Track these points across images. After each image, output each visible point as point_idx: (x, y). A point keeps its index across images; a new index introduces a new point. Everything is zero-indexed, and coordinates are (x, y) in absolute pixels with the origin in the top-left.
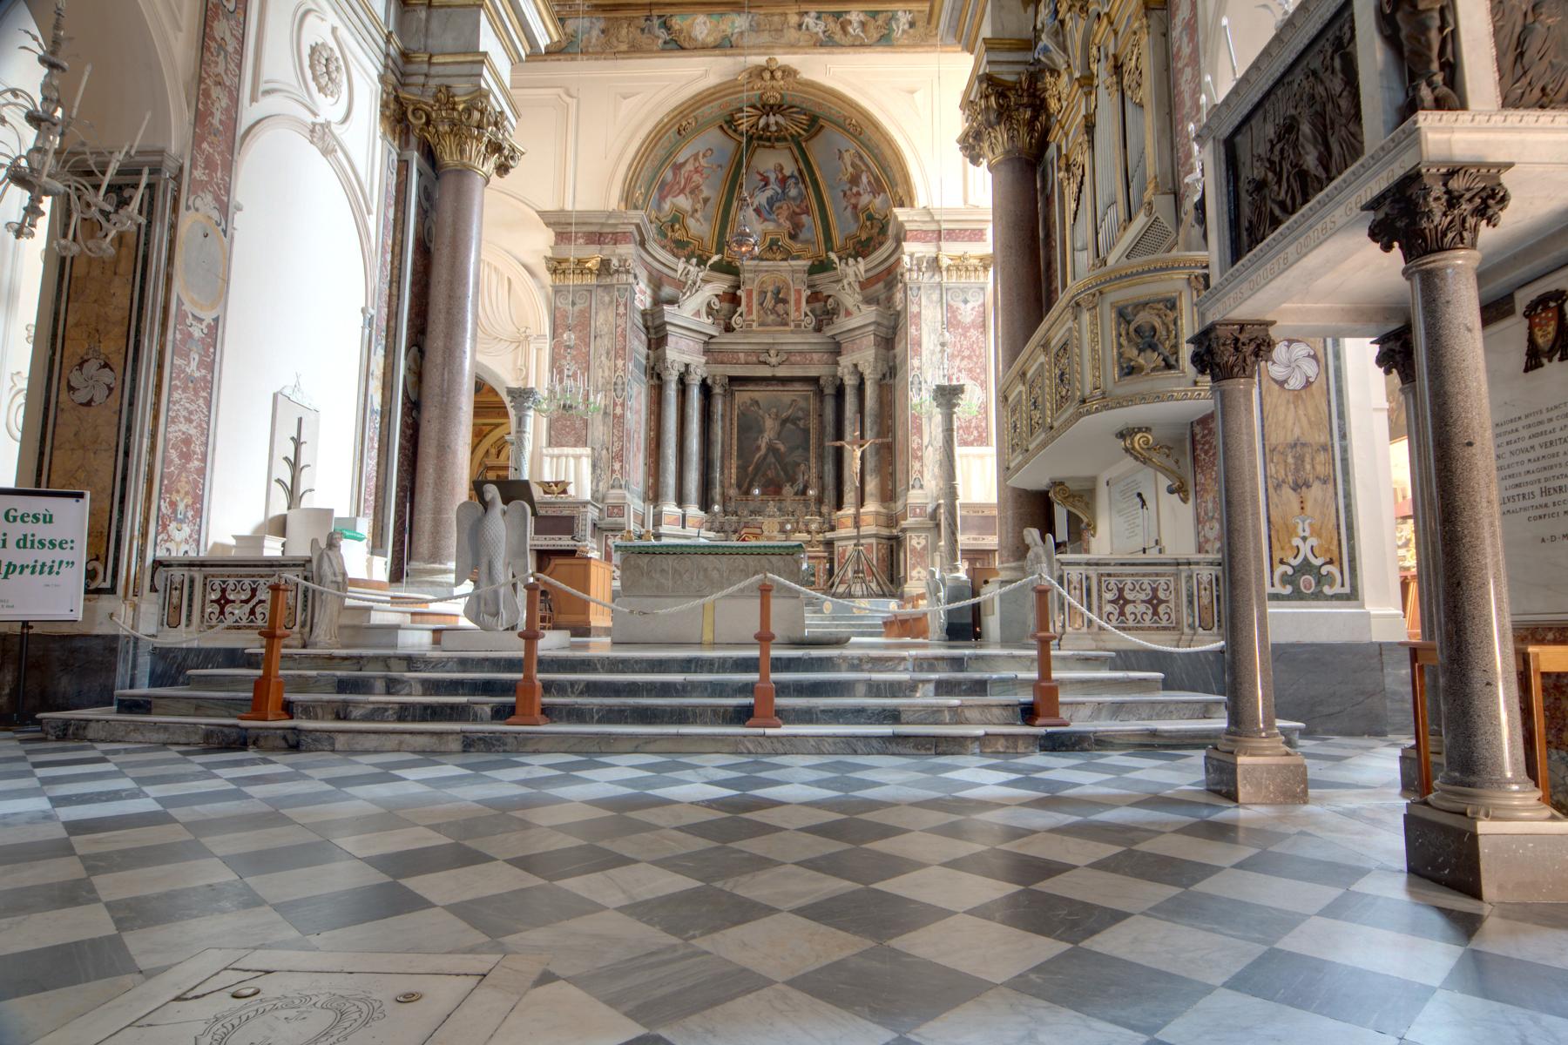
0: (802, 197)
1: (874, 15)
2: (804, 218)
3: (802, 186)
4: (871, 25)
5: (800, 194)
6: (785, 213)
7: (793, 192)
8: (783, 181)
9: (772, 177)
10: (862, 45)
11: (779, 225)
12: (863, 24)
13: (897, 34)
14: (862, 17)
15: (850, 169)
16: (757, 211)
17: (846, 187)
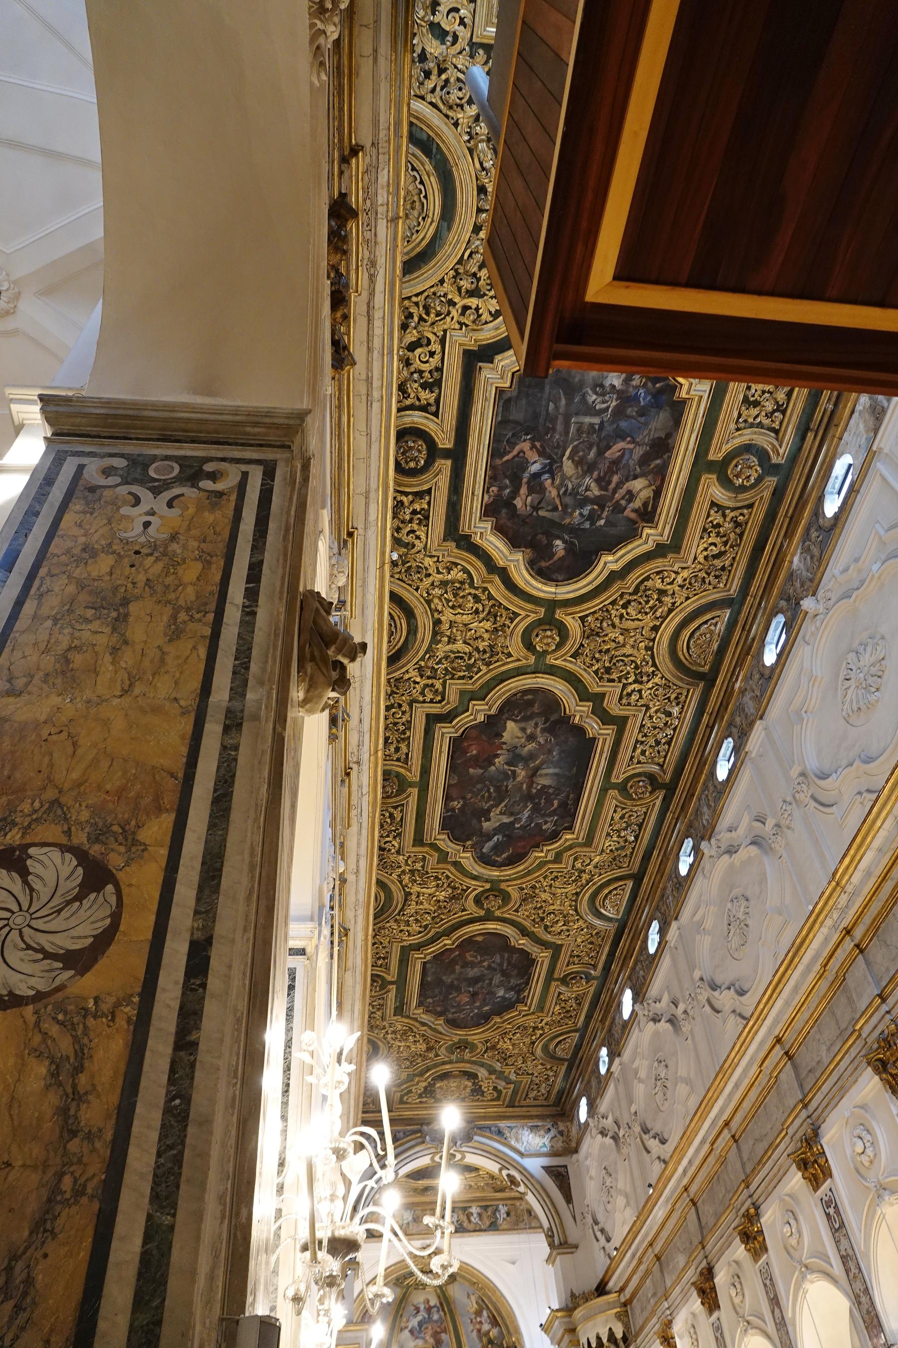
0: (441, 1320)
1: (485, 1208)
2: (443, 1336)
3: (442, 1313)
4: (485, 1215)
5: (441, 1317)
6: (430, 1332)
7: (436, 1317)
8: (429, 1310)
9: (422, 1307)
10: (480, 1230)
11: (426, 1341)
12: (480, 1215)
13: (500, 1221)
14: (479, 1210)
15: (475, 1306)
16: (411, 1332)
17: (473, 1316)
